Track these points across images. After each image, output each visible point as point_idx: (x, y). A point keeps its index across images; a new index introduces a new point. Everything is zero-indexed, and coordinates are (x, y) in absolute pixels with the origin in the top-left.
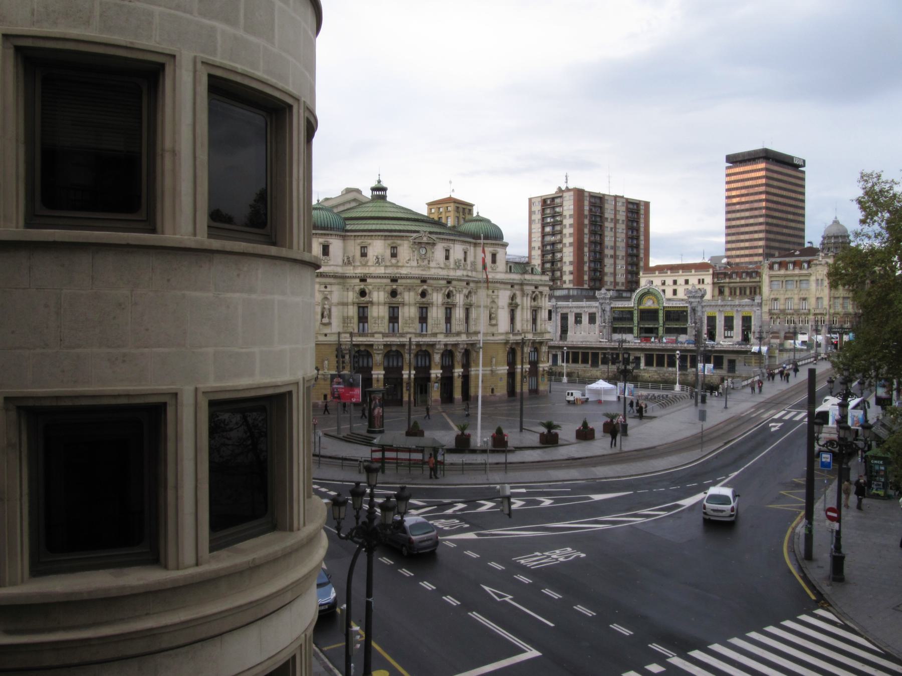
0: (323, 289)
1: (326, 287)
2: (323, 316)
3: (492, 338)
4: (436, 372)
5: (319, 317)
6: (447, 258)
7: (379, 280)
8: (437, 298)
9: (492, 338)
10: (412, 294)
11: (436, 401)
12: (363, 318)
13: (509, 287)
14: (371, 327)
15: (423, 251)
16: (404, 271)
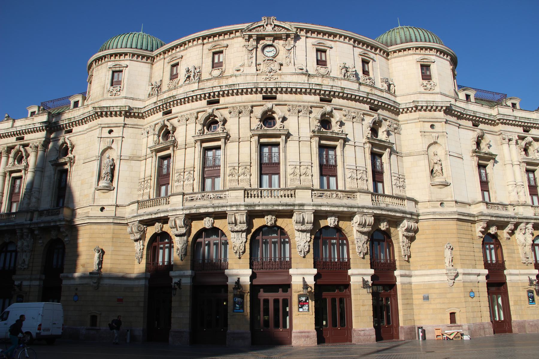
0: (108, 135)
1: (110, 132)
2: (99, 177)
3: (440, 209)
4: (302, 275)
5: (95, 178)
6: (321, 63)
7: (188, 106)
8: (301, 127)
9: (440, 209)
10: (245, 120)
11: (304, 335)
12: (163, 178)
13: (470, 124)
14: (175, 186)
15: (270, 52)
16: (230, 81)
